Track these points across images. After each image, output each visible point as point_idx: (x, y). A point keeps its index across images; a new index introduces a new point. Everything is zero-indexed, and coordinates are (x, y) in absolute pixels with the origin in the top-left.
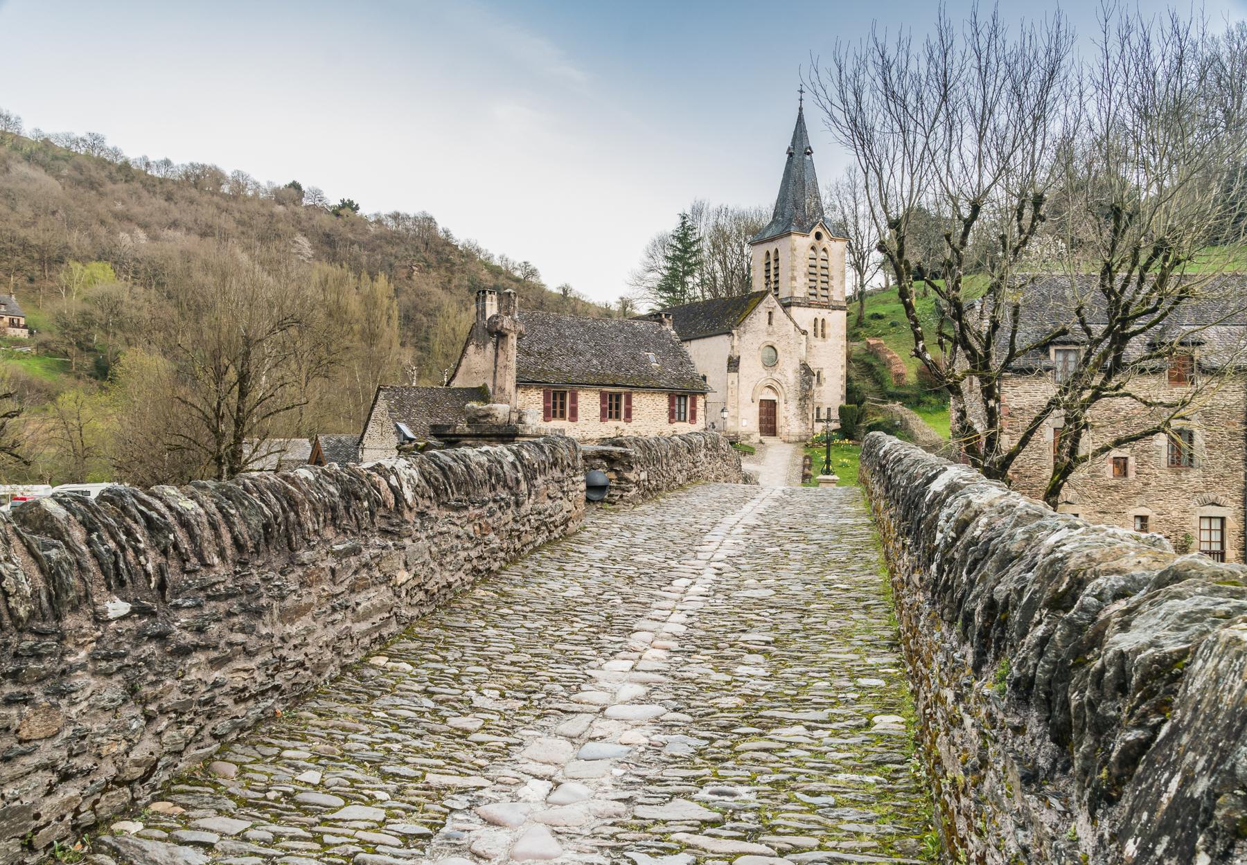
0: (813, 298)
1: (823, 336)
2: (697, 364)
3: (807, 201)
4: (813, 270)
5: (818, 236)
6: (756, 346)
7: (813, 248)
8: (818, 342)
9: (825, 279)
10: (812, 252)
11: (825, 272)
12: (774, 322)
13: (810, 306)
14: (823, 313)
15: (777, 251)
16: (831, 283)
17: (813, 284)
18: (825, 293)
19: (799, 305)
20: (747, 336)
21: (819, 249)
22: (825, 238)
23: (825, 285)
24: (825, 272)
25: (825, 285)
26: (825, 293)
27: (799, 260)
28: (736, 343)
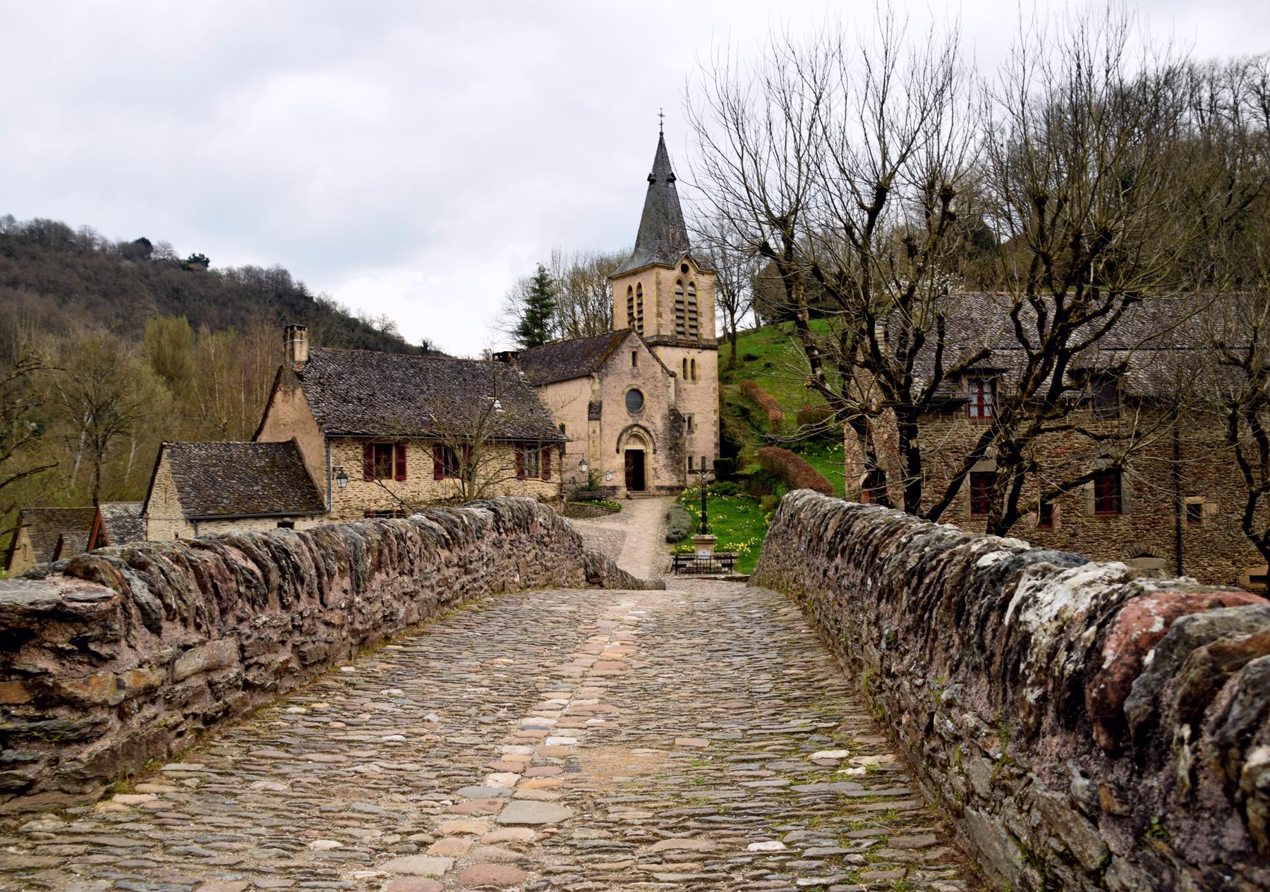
0: (680, 337)
1: (693, 378)
4: (680, 307)
5: (685, 269)
6: (619, 390)
8: (688, 385)
9: (693, 316)
12: (639, 363)
13: (677, 346)
14: (693, 354)
15: (639, 286)
16: (701, 319)
18: (693, 331)
19: (665, 344)
20: (609, 379)
21: (686, 282)
22: (692, 271)
23: (693, 323)
25: (693, 323)
26: (693, 331)
27: (664, 295)
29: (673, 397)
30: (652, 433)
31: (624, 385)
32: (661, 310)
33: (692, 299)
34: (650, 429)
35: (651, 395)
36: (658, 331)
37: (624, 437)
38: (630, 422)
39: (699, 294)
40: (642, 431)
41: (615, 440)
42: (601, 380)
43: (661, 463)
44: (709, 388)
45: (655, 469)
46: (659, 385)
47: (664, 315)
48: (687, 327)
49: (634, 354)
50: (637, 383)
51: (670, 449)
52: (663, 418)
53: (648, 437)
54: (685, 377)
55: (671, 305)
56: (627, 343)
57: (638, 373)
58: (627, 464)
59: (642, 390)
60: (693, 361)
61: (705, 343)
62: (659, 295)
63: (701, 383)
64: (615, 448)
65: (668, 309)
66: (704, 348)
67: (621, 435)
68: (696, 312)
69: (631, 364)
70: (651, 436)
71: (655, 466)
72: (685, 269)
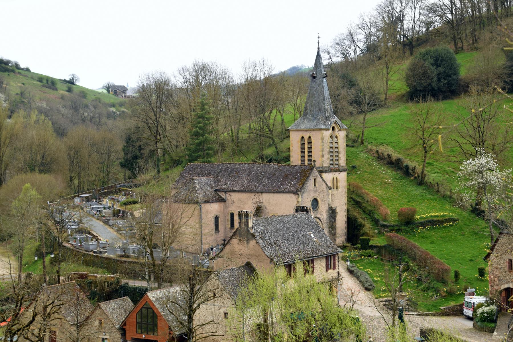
0: (332, 166)
1: (337, 188)
2: (268, 208)
3: (326, 107)
4: (331, 150)
5: (333, 129)
9: (337, 154)
10: (330, 139)
12: (317, 185)
13: (331, 171)
14: (336, 175)
15: (310, 137)
17: (332, 158)
18: (337, 162)
19: (326, 172)
20: (305, 195)
21: (334, 137)
22: (336, 130)
23: (337, 158)
24: (336, 150)
25: (337, 158)
26: (337, 162)
27: (325, 145)
28: (300, 199)
29: (330, 201)
32: (324, 153)
33: (336, 145)
34: (321, 219)
35: (322, 201)
36: (323, 165)
39: (339, 142)
40: (318, 220)
42: (302, 196)
46: (325, 195)
47: (325, 156)
48: (334, 161)
49: (315, 179)
50: (316, 195)
51: (329, 228)
52: (326, 212)
53: (320, 223)
55: (328, 149)
56: (312, 175)
57: (317, 190)
59: (318, 199)
61: (341, 168)
62: (323, 145)
63: (340, 190)
65: (326, 152)
68: (338, 152)
69: (314, 185)
70: (322, 222)
72: (333, 129)
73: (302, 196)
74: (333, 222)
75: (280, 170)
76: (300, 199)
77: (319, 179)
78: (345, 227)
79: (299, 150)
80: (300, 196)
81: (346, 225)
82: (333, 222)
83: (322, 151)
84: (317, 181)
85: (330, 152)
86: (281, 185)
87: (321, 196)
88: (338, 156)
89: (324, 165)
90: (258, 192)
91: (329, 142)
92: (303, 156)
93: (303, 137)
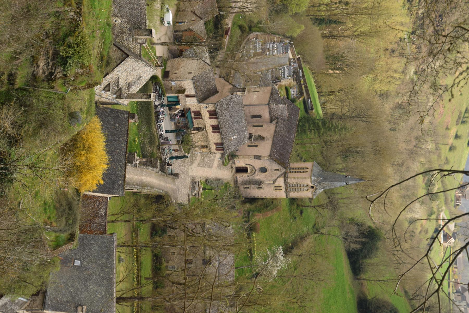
0: (288, 185)
1: (276, 189)
3: (326, 183)
4: (299, 186)
5: (312, 187)
6: (266, 165)
7: (307, 185)
8: (273, 188)
9: (297, 190)
10: (306, 185)
11: (299, 190)
12: (275, 171)
13: (285, 184)
14: (284, 190)
15: (307, 172)
16: (296, 192)
17: (294, 186)
18: (291, 190)
19: (285, 180)
20: (269, 162)
22: (312, 190)
23: (294, 190)
24: (299, 190)
25: (294, 190)
26: (291, 190)
27: (302, 180)
28: (266, 158)
30: (254, 175)
31: (268, 167)
32: (296, 179)
33: (302, 190)
34: (255, 175)
35: (266, 175)
36: (289, 178)
37: (251, 166)
38: (256, 169)
39: (305, 192)
40: (254, 172)
41: (250, 164)
42: (268, 159)
43: (245, 178)
44: (273, 195)
45: (242, 176)
46: (270, 178)
48: (292, 188)
49: (279, 170)
50: (269, 170)
52: (259, 179)
54: (275, 187)
56: (282, 168)
57: (272, 171)
58: (243, 167)
59: (267, 172)
60: (281, 189)
61: (288, 193)
62: (301, 178)
63: (274, 192)
64: (247, 163)
65: (297, 181)
66: (286, 193)
67: (251, 165)
70: (253, 175)
71: (243, 176)
72: (312, 187)
73: (268, 159)
74: (253, 183)
75: (287, 153)
76: (266, 158)
77: (279, 173)
78: (251, 196)
79: (300, 167)
80: (268, 158)
81: (252, 197)
82: (253, 183)
83: (297, 178)
84: (278, 172)
85: (297, 184)
86: (277, 151)
87: (269, 175)
88: (295, 191)
89: (289, 179)
90: (273, 138)
91: (304, 183)
92: (296, 169)
93: (308, 168)
